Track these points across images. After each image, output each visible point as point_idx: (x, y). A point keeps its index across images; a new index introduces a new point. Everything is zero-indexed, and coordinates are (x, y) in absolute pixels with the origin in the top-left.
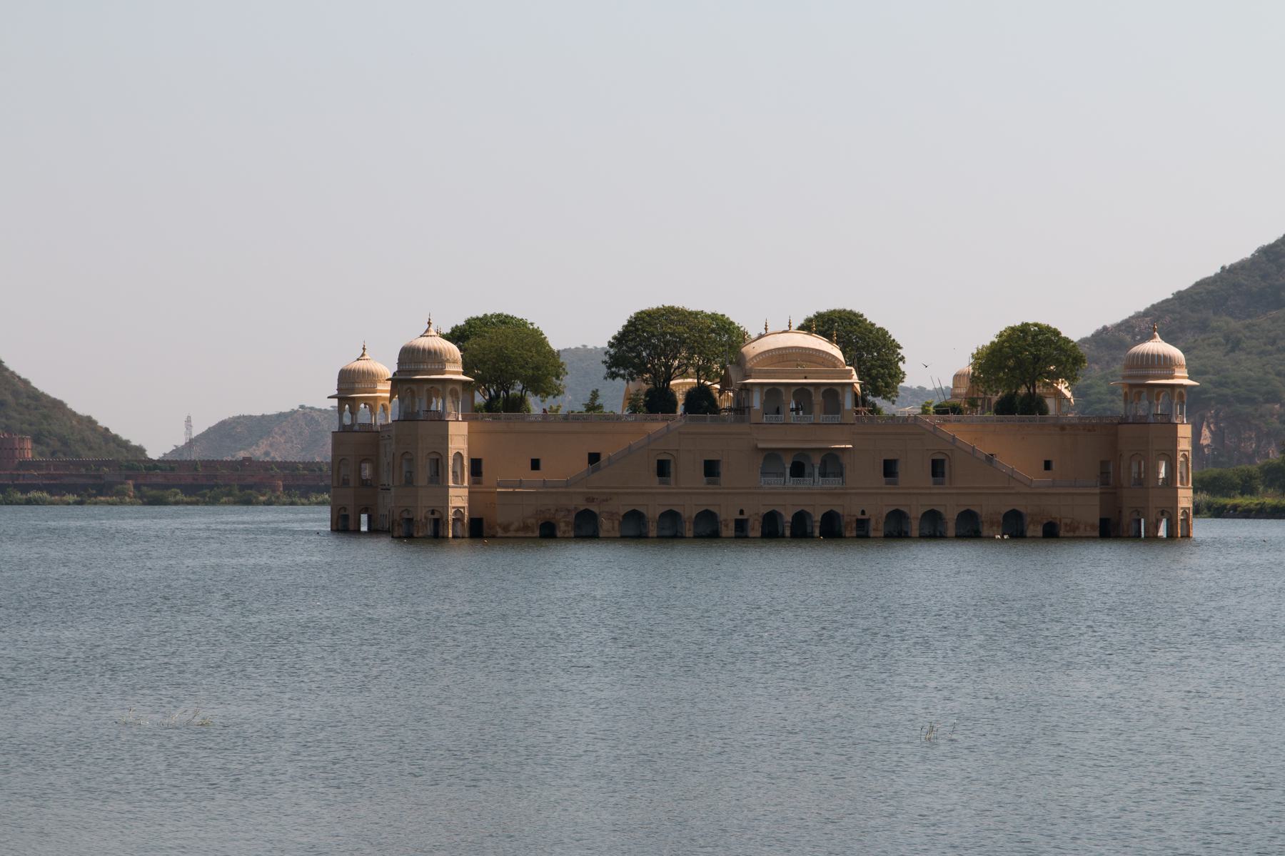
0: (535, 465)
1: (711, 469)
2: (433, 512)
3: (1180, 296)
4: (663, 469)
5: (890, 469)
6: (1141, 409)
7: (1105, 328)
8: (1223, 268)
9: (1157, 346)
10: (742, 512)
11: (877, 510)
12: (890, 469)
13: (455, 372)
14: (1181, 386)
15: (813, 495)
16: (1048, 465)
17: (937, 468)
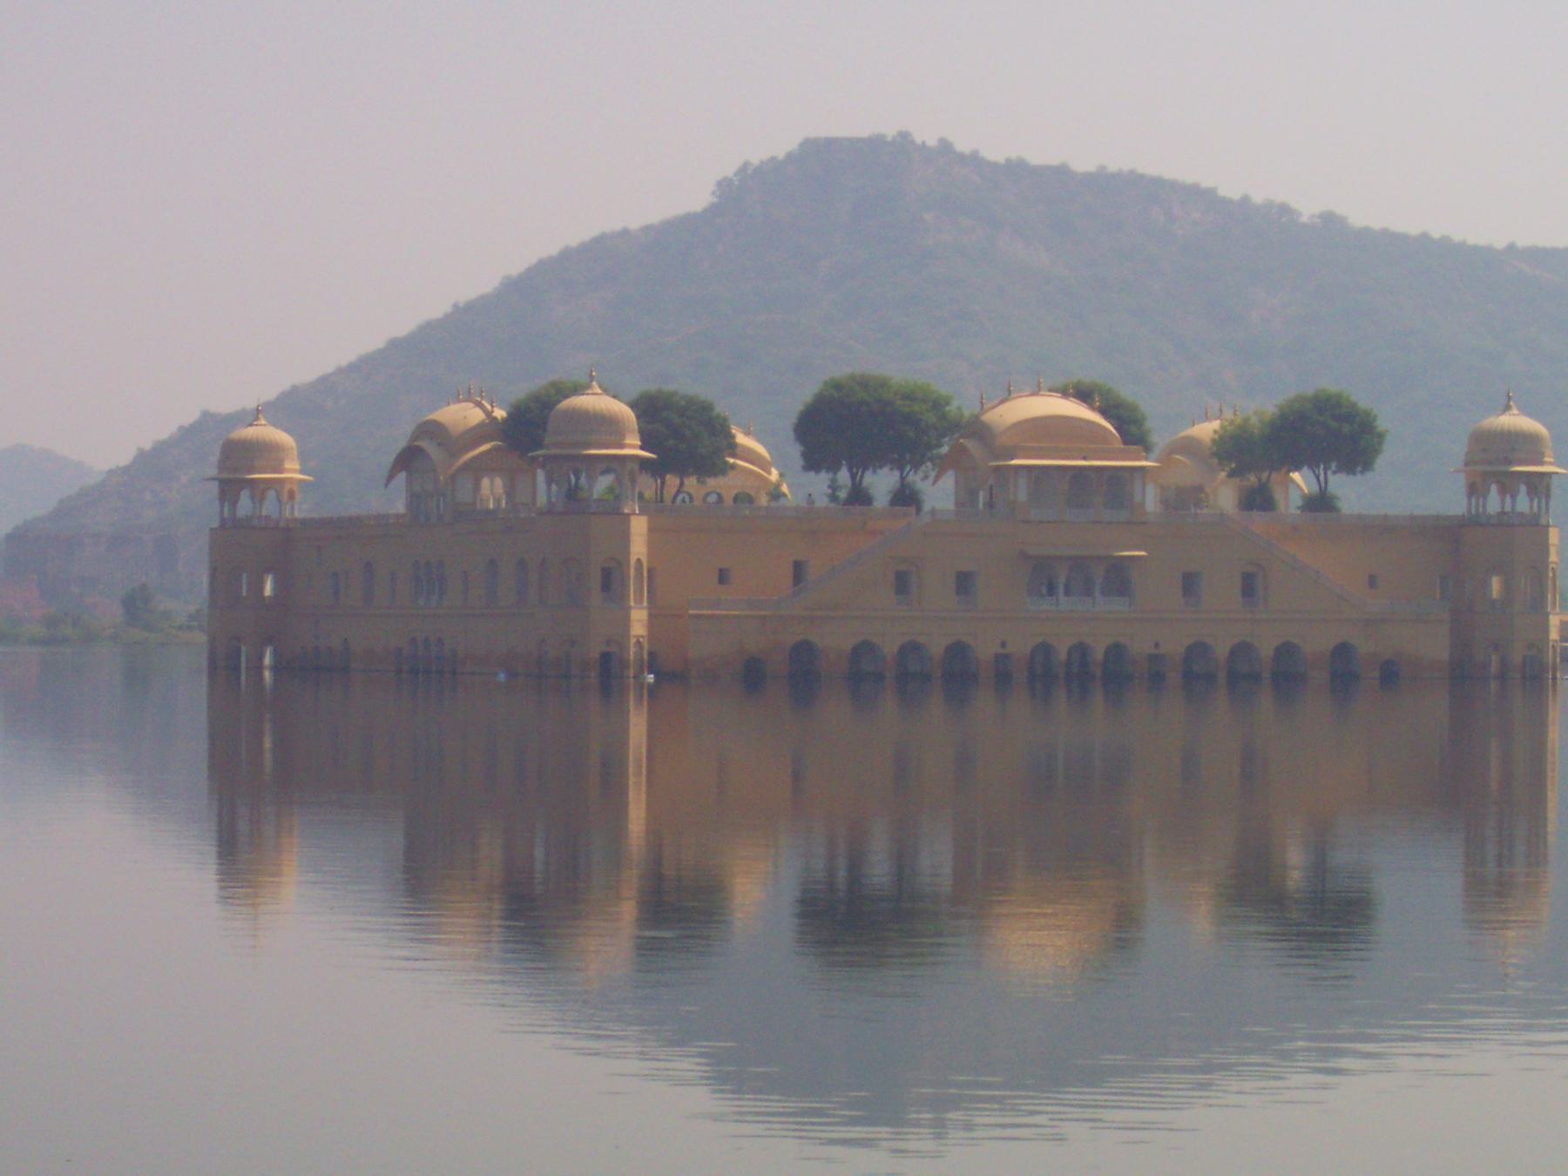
0: (723, 577)
1: (964, 583)
2: (608, 642)
3: (394, 344)
4: (902, 584)
5: (1189, 583)
6: (1493, 503)
7: (294, 390)
8: (455, 306)
9: (1515, 420)
10: (1003, 645)
11: (1174, 644)
12: (1189, 583)
13: (632, 447)
14: (1550, 474)
15: (1088, 622)
16: (1372, 581)
17: (1248, 587)
